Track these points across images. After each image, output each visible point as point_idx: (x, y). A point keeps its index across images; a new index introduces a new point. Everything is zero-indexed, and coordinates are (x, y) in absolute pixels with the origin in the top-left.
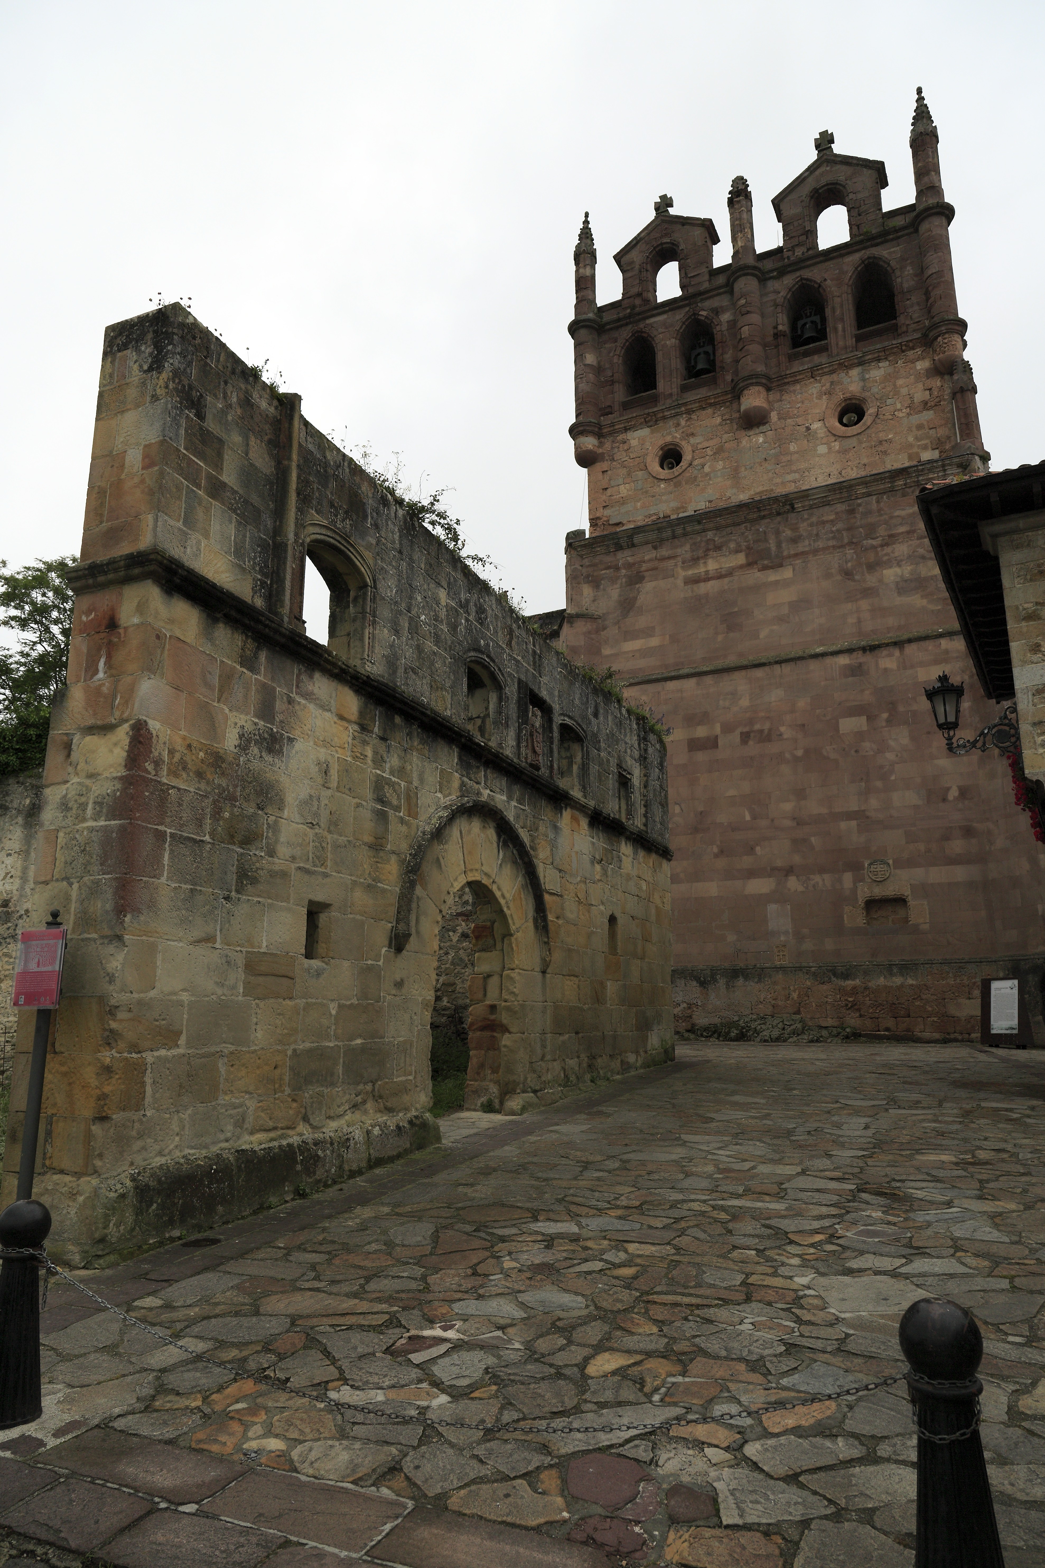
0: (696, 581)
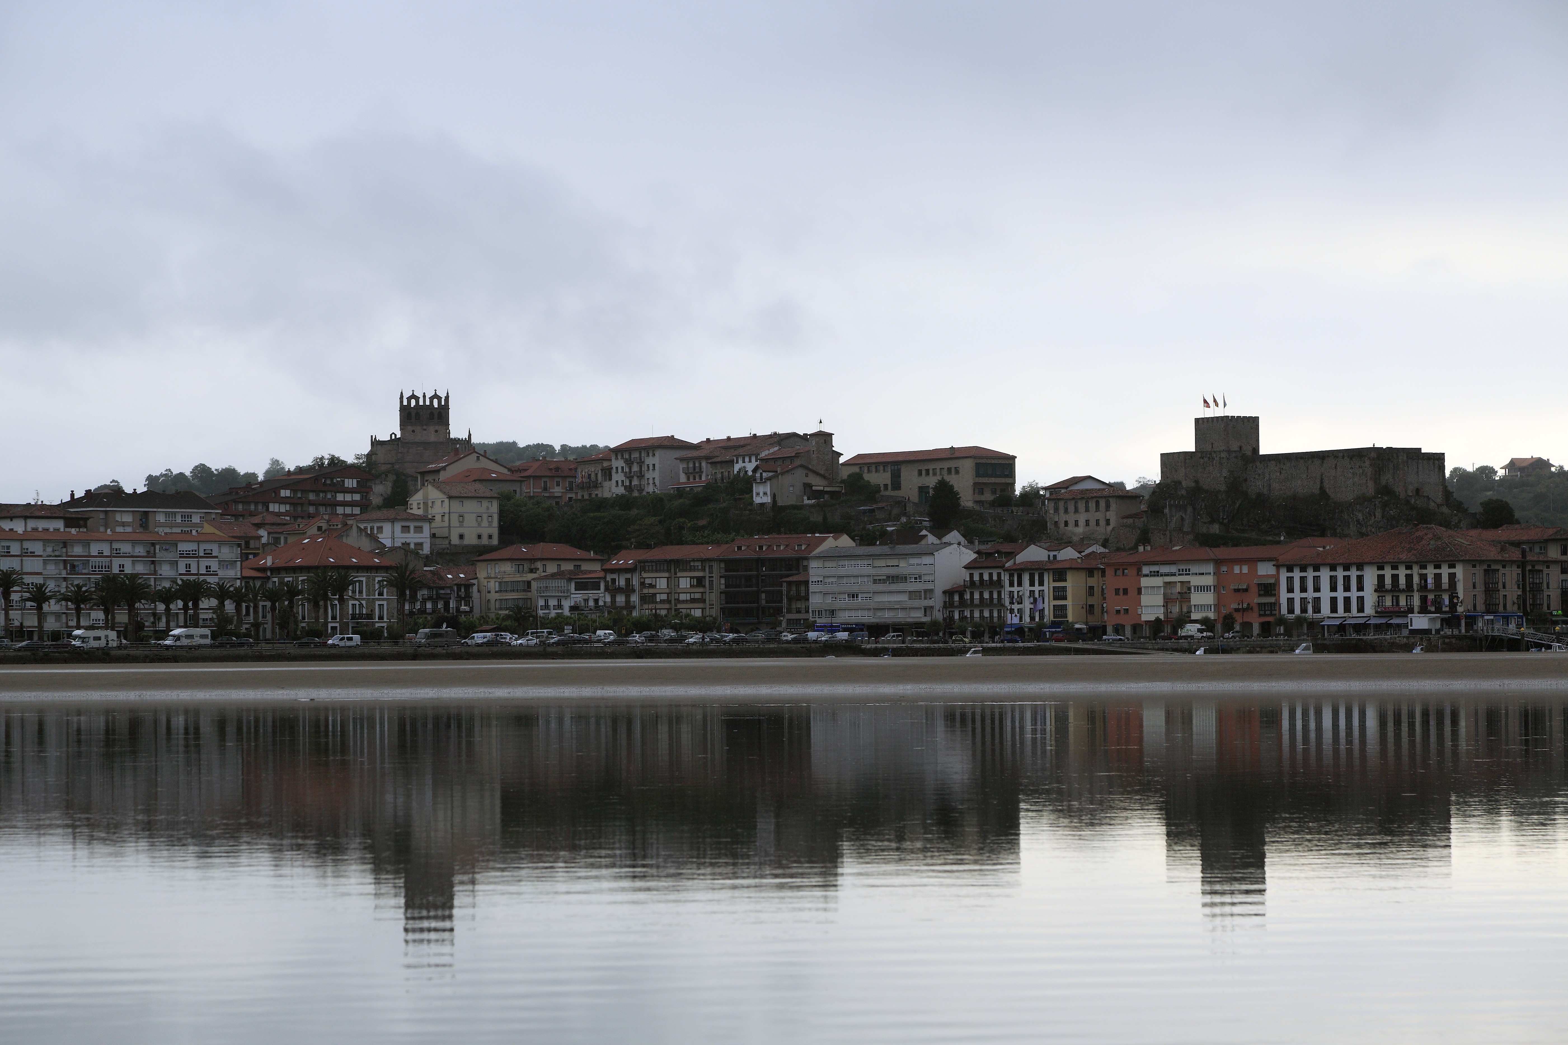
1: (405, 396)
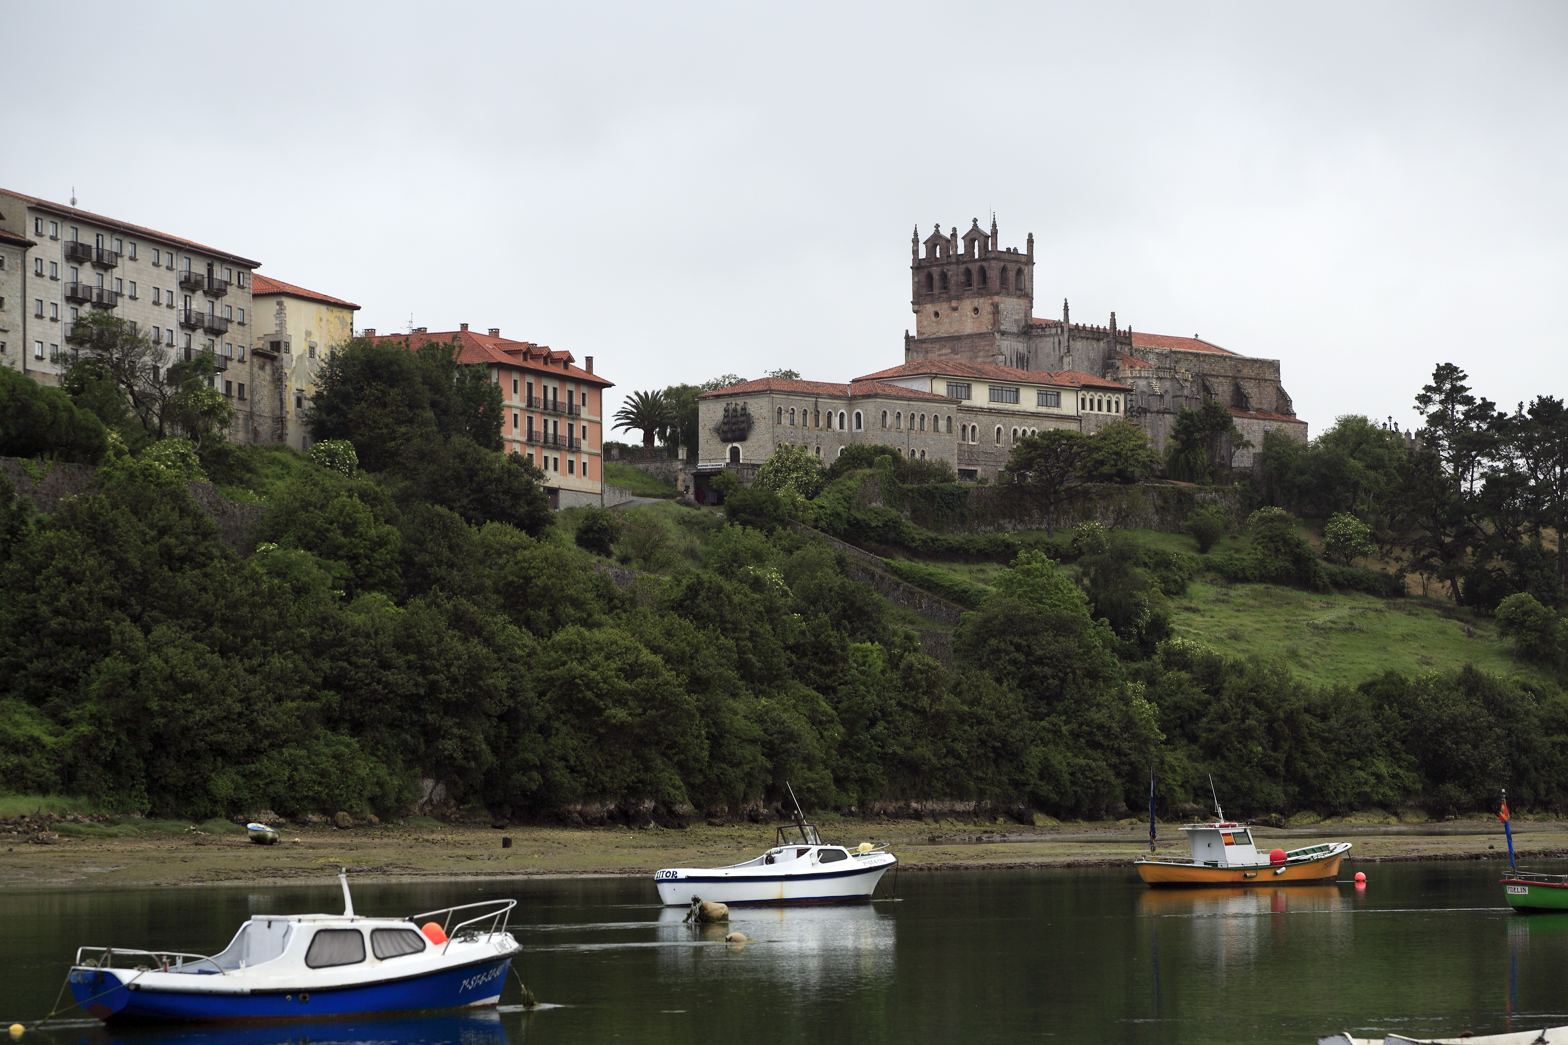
0: (940, 355)
1: (923, 238)
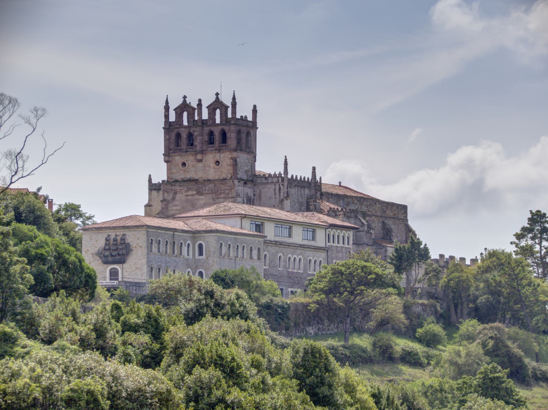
0: (187, 196)
1: (173, 105)
